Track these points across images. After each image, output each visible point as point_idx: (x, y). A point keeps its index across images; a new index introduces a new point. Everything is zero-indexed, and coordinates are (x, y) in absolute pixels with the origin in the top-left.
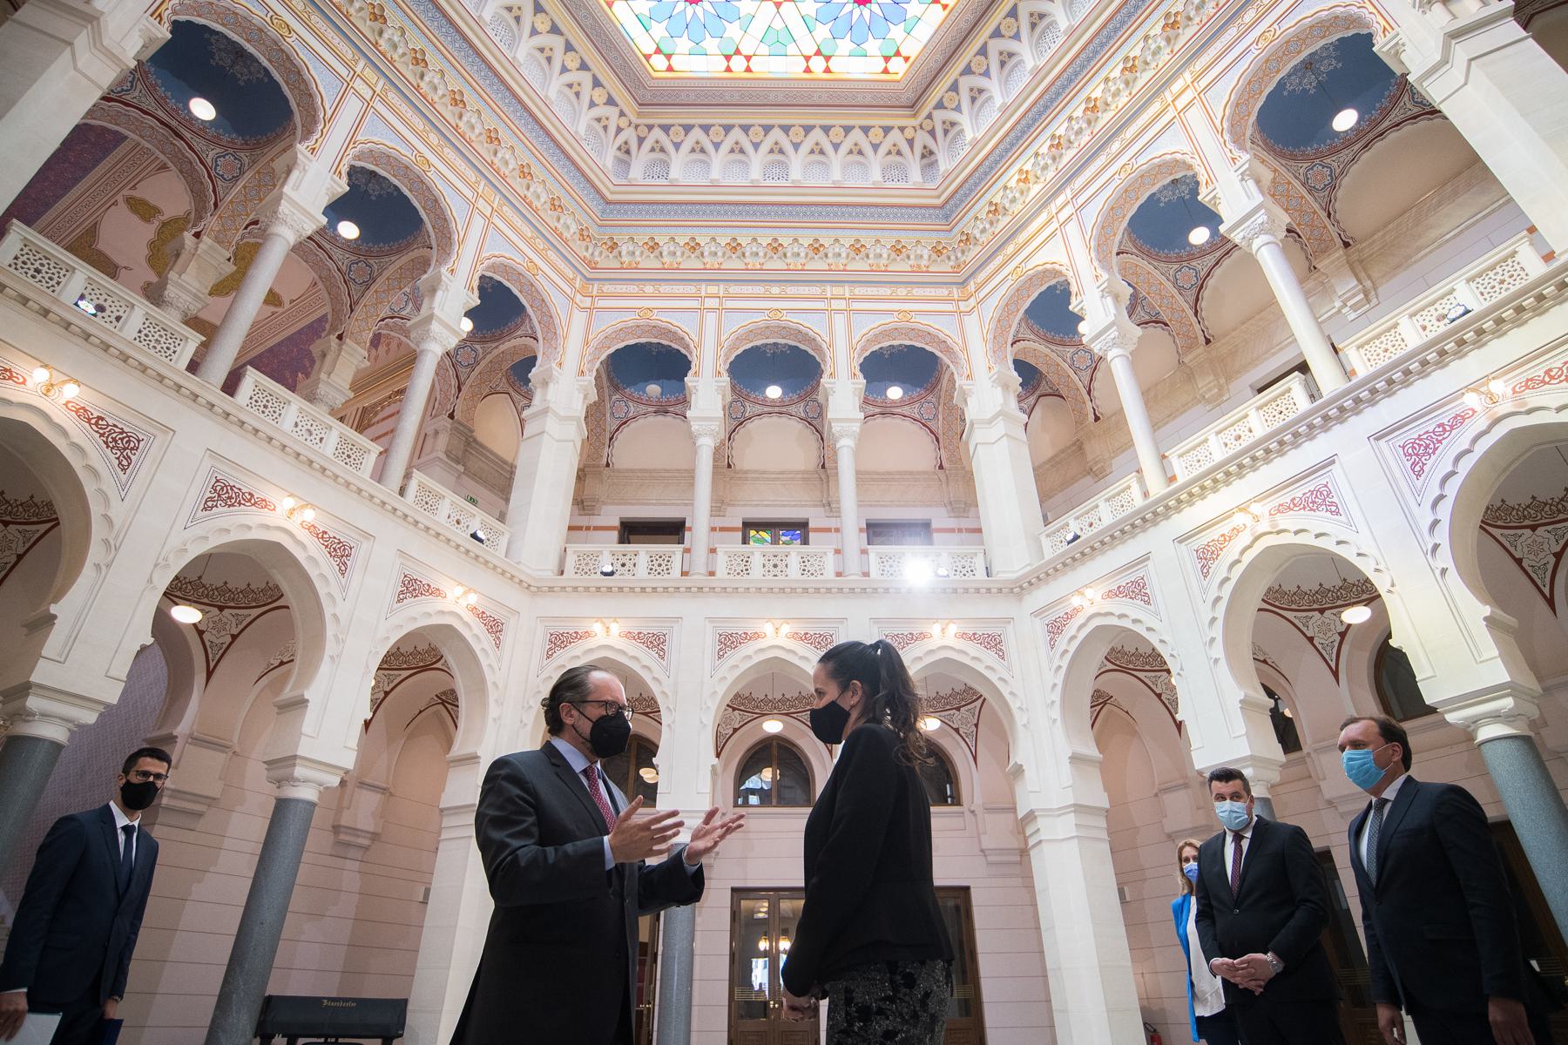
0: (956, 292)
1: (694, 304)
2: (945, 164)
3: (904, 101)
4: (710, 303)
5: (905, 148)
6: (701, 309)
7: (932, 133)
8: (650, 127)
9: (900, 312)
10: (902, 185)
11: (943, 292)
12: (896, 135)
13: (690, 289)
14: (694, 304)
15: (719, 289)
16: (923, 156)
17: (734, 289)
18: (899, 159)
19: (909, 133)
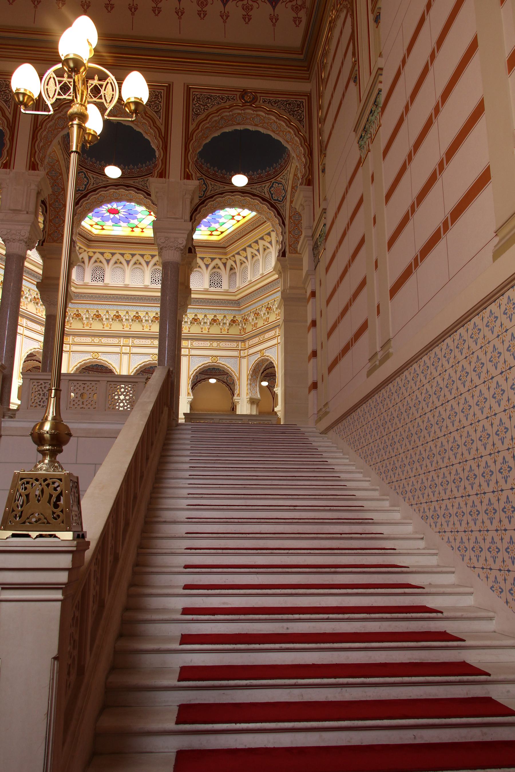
0: (241, 345)
1: (117, 350)
2: (239, 284)
3: (221, 245)
4: (125, 350)
5: (222, 266)
6: (121, 353)
7: (235, 262)
8: (94, 253)
9: (212, 356)
10: (218, 289)
11: (234, 345)
12: (217, 261)
13: (115, 341)
14: (117, 350)
15: (130, 341)
16: (231, 269)
17: (137, 342)
18: (218, 270)
19: (224, 261)
